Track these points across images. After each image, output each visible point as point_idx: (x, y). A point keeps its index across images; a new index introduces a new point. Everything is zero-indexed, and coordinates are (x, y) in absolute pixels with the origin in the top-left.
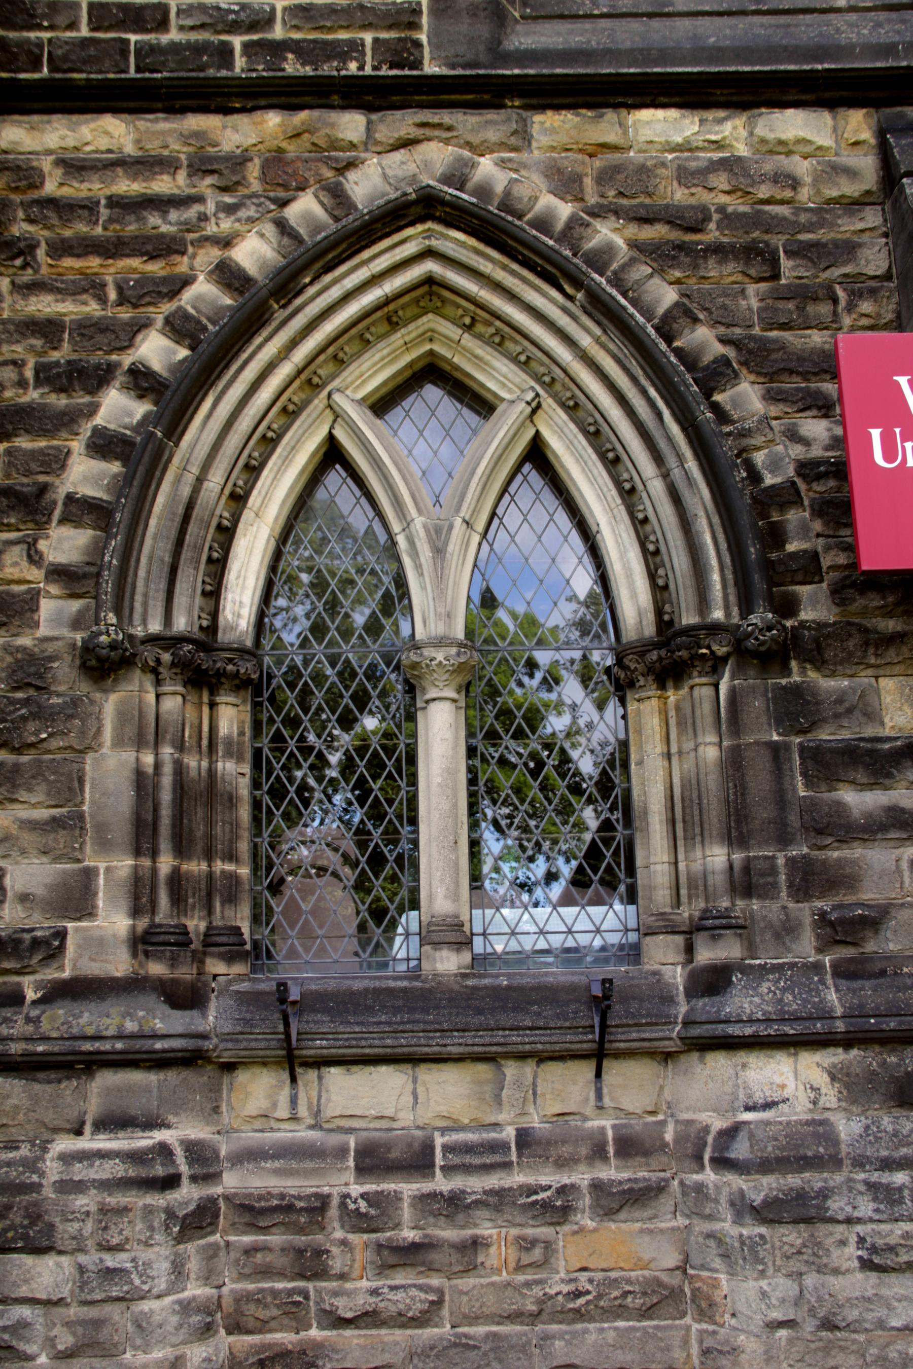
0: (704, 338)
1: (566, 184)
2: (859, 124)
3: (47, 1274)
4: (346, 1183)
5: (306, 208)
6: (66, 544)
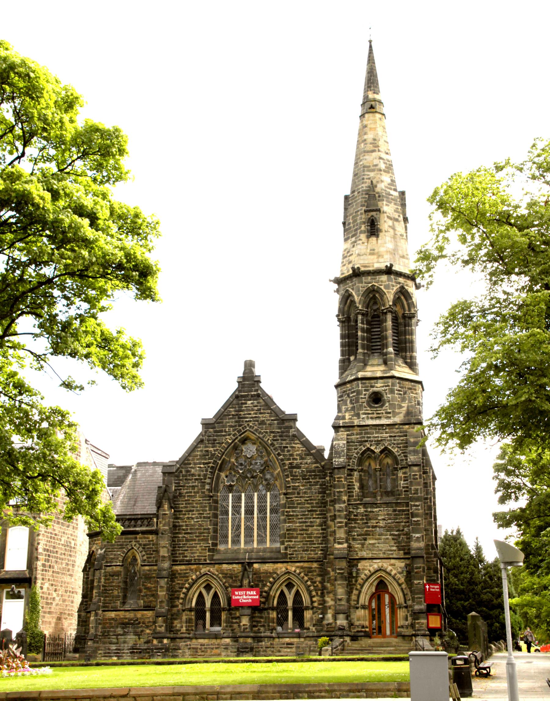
0: (227, 584)
1: (217, 571)
2: (240, 565)
3: (180, 651)
4: (199, 647)
5: (198, 573)
6: (181, 601)
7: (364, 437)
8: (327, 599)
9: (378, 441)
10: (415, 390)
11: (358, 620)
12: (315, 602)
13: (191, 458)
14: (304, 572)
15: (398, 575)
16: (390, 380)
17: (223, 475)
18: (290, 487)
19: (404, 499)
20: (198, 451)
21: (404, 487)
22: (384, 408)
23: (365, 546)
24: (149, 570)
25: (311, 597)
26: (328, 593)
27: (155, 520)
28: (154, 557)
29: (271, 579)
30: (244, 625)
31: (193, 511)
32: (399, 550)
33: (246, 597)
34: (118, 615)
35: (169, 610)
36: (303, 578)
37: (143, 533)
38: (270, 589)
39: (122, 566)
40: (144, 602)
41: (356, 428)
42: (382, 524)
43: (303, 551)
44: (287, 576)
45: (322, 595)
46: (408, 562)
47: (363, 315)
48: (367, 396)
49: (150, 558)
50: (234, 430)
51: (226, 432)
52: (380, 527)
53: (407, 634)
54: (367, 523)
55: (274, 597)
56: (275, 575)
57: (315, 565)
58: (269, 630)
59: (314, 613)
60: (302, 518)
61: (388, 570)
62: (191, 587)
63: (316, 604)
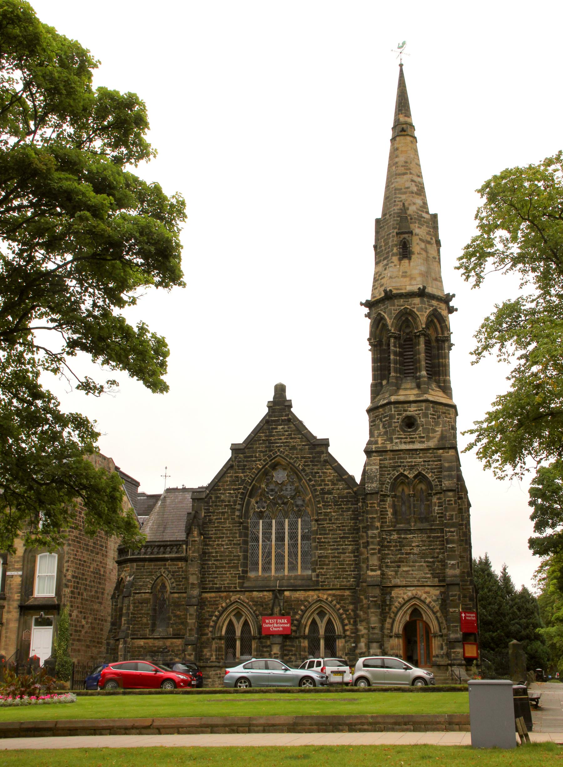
0: (257, 612)
1: (248, 599)
2: (271, 593)
3: (210, 680)
5: (228, 601)
6: (211, 629)
7: (397, 462)
8: (360, 627)
9: (412, 466)
10: (449, 414)
11: (392, 649)
12: (347, 630)
13: (220, 484)
14: (337, 599)
15: (433, 603)
16: (424, 404)
17: (253, 501)
18: (321, 513)
19: (438, 525)
20: (228, 477)
21: (438, 513)
22: (417, 432)
23: (399, 573)
24: (179, 598)
25: (344, 625)
26: (361, 621)
27: (184, 546)
28: (183, 585)
29: (302, 607)
30: (275, 654)
31: (223, 537)
32: (434, 577)
33: (277, 625)
34: (147, 643)
35: (198, 639)
36: (335, 606)
37: (172, 559)
38: (302, 617)
39: (151, 593)
40: (173, 630)
41: (389, 453)
42: (416, 550)
43: (335, 578)
44: (318, 604)
45: (355, 623)
46: (443, 589)
47: (395, 338)
48: (399, 420)
49: (180, 585)
50: (264, 456)
51: (256, 457)
52: (414, 554)
53: (442, 663)
54: (401, 550)
55: (306, 626)
56: (306, 603)
57: (347, 593)
58: (300, 659)
59: (346, 642)
60: (334, 545)
61: (422, 598)
62: (221, 614)
63: (348, 633)
